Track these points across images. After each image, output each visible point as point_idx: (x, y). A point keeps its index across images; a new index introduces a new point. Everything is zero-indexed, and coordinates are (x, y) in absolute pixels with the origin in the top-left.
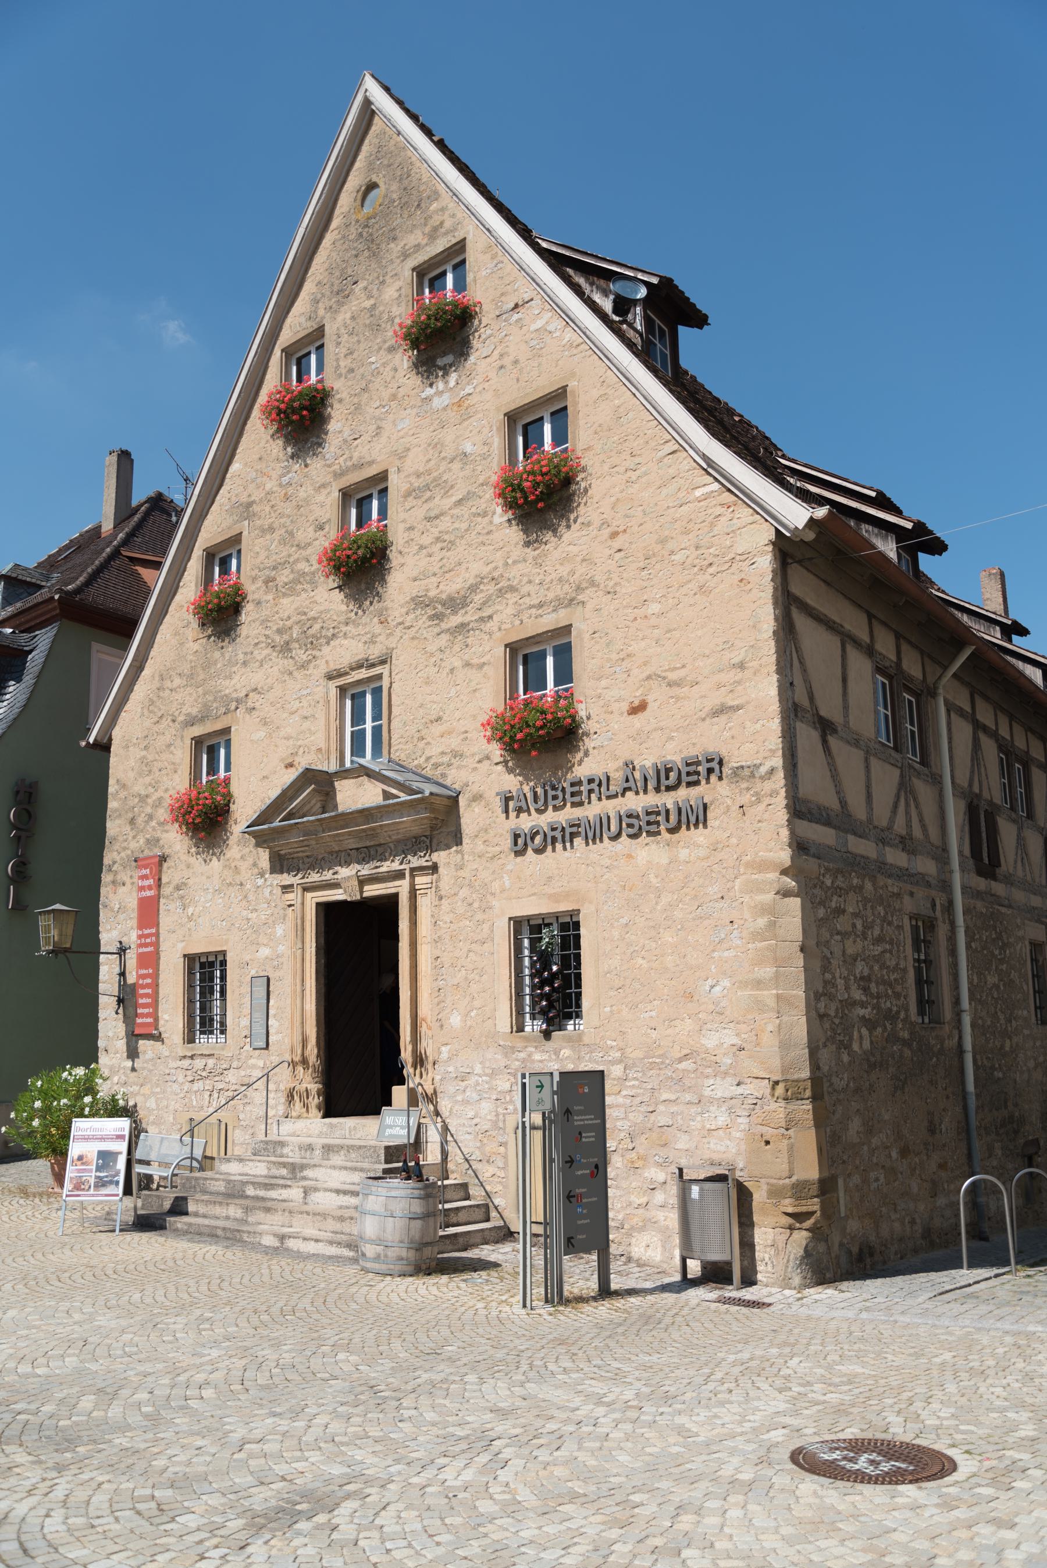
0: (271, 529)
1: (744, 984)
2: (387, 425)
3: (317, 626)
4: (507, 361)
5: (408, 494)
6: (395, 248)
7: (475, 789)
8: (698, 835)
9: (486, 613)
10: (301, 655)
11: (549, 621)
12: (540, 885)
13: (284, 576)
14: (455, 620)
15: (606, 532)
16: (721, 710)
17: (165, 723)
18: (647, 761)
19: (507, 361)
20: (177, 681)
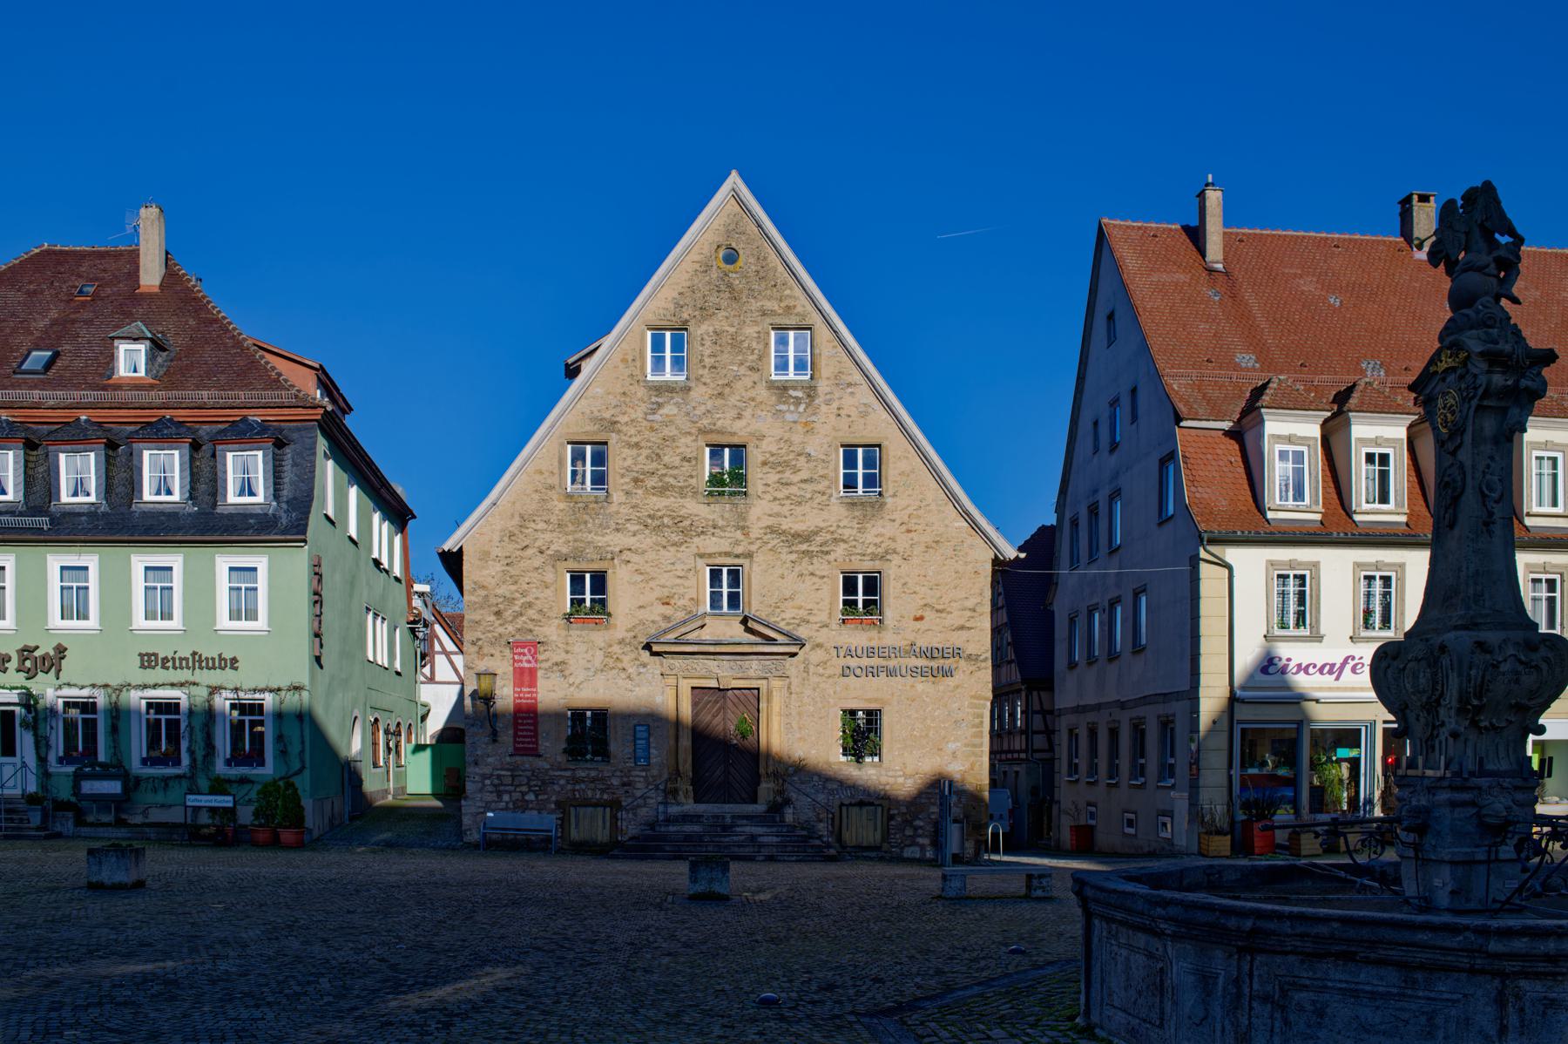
0: (637, 445)
1: (966, 745)
2: (747, 413)
3: (687, 523)
4: (843, 412)
5: (764, 463)
6: (755, 305)
7: (819, 640)
8: (950, 682)
9: (825, 549)
10: (675, 538)
11: (868, 565)
12: (861, 695)
13: (651, 482)
14: (804, 547)
15: (904, 528)
16: (962, 628)
17: (529, 552)
18: (923, 642)
19: (843, 412)
20: (541, 526)
